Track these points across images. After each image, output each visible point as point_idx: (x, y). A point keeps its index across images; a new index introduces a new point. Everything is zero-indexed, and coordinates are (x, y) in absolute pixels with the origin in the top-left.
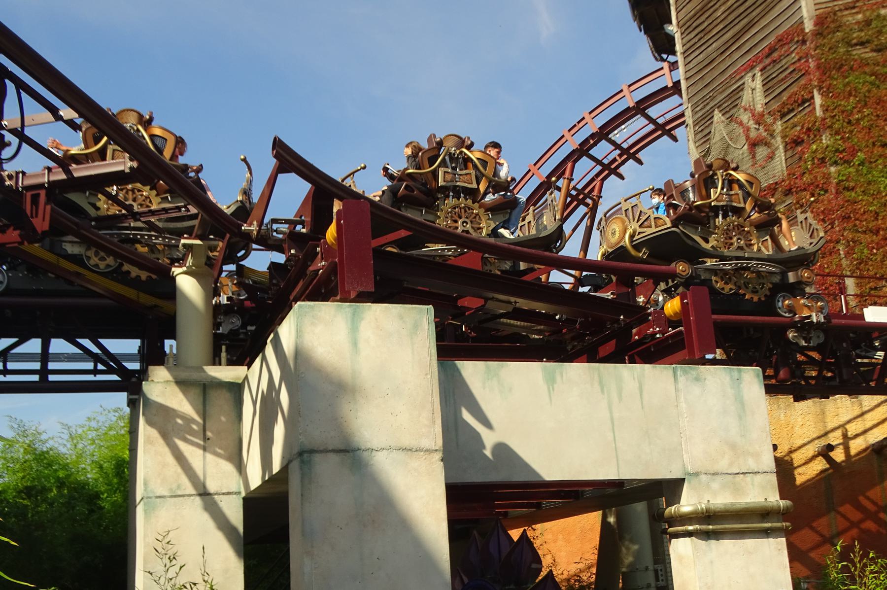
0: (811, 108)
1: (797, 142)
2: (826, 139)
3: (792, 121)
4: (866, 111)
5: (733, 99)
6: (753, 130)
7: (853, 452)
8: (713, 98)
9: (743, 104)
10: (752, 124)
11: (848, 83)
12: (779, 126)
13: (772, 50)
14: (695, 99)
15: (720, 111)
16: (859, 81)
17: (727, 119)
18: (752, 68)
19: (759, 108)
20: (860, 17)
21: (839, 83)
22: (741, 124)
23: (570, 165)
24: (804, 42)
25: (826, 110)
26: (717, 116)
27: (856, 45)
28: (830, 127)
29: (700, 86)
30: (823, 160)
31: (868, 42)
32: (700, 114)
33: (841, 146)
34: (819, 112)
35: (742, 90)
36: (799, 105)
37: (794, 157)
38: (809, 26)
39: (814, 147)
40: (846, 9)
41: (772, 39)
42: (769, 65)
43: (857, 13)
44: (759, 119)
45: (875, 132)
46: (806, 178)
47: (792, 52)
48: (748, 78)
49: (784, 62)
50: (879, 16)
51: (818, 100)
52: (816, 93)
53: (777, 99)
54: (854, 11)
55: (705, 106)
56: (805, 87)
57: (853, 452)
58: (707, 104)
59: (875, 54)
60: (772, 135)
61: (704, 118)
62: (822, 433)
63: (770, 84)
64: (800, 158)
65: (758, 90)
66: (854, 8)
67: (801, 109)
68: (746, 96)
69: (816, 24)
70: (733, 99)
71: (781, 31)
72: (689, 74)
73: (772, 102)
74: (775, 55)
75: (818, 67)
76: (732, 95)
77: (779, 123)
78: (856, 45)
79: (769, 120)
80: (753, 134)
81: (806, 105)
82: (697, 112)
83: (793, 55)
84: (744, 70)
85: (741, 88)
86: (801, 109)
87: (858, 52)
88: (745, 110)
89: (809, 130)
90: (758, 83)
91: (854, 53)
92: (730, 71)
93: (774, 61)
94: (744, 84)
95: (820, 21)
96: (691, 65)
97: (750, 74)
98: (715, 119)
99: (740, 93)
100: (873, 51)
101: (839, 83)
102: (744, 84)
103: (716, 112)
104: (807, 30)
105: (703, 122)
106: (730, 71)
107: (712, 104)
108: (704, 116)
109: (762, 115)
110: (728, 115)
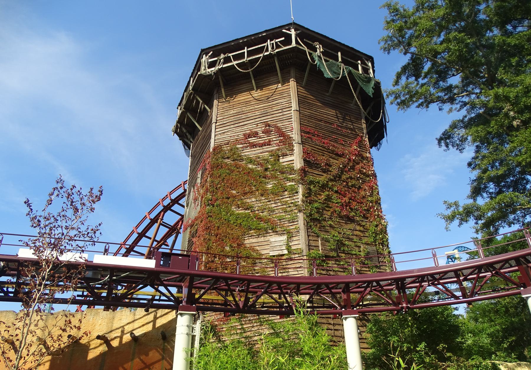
7: (124, 342)
23: (162, 213)
27: (226, 158)
57: (124, 342)
62: (110, 330)
78: (226, 158)
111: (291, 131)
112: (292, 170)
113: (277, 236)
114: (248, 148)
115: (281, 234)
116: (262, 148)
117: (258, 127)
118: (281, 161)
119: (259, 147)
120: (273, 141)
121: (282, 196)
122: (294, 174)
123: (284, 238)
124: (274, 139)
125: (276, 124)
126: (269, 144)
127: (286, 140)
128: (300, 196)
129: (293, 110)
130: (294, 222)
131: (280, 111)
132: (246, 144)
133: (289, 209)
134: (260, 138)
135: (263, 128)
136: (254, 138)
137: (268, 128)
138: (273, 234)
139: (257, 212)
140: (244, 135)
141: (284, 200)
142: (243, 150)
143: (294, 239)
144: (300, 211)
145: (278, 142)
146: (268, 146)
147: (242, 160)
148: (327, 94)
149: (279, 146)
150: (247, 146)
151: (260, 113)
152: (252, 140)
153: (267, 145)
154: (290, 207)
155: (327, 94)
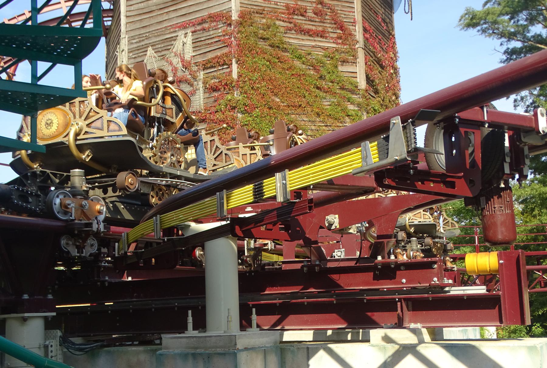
0: (228, 70)
1: (215, 89)
2: (237, 95)
3: (212, 74)
4: (264, 84)
5: (166, 44)
6: (179, 70)
8: (148, 38)
9: (174, 50)
10: (180, 66)
11: (255, 62)
12: (201, 75)
13: (203, 21)
14: (133, 34)
15: (153, 49)
16: (261, 63)
17: (159, 56)
18: (185, 28)
19: (188, 57)
20: (264, 21)
21: (249, 61)
22: (171, 64)
24: (230, 25)
25: (240, 76)
26: (150, 51)
27: (261, 38)
28: (242, 88)
29: (138, 25)
30: (234, 108)
31: (268, 39)
32: (135, 45)
33: (248, 102)
34: (235, 75)
35: (175, 40)
36: (219, 65)
37: (210, 99)
38: (235, 16)
39: (230, 98)
40: (257, 13)
41: (205, 13)
42: (199, 30)
43: (263, 18)
44: (186, 66)
45: (266, 97)
46: (219, 116)
47: (219, 28)
48: (181, 33)
49: (211, 33)
50: (275, 24)
51: (235, 66)
52: (234, 61)
53: (202, 55)
54: (262, 16)
55: (140, 41)
56: (226, 55)
58: (143, 40)
59: (270, 48)
60: (195, 78)
61: (138, 50)
63: (198, 44)
64: (215, 101)
65: (188, 45)
66: (262, 14)
67: (220, 68)
68: (178, 46)
69: (240, 17)
70: (166, 44)
71: (213, 11)
72: (129, 14)
73: (198, 56)
74: (206, 25)
75: (238, 45)
76: (165, 41)
77: (202, 73)
78: (261, 38)
79: (195, 68)
80: (180, 74)
81: (225, 67)
82: (132, 43)
83: (220, 31)
84: (179, 27)
85: (175, 39)
86: (220, 68)
87: (261, 44)
88: (176, 55)
89: (226, 84)
90: (189, 39)
91: (260, 43)
92: (165, 24)
93: (204, 30)
94: (177, 36)
95: (242, 15)
96: (132, 8)
97: (183, 32)
98: (148, 53)
99: (173, 42)
100: (270, 46)
101: (249, 61)
102: (177, 36)
103: (150, 49)
104: (233, 18)
105: (137, 52)
106: (165, 24)
107: (146, 42)
108: (139, 48)
109: (190, 63)
110: (160, 54)
111: (354, 23)
112: (354, 89)
114: (293, 32)
116: (312, 38)
118: (340, 68)
119: (310, 36)
120: (328, 32)
121: (341, 122)
124: (330, 30)
125: (334, 5)
126: (322, 35)
132: (290, 23)
134: (309, 20)
135: (314, 6)
136: (300, 17)
137: (320, 6)
140: (287, 7)
142: (286, 33)
147: (285, 50)
149: (337, 44)
150: (290, 30)
152: (298, 19)
153: (321, 37)
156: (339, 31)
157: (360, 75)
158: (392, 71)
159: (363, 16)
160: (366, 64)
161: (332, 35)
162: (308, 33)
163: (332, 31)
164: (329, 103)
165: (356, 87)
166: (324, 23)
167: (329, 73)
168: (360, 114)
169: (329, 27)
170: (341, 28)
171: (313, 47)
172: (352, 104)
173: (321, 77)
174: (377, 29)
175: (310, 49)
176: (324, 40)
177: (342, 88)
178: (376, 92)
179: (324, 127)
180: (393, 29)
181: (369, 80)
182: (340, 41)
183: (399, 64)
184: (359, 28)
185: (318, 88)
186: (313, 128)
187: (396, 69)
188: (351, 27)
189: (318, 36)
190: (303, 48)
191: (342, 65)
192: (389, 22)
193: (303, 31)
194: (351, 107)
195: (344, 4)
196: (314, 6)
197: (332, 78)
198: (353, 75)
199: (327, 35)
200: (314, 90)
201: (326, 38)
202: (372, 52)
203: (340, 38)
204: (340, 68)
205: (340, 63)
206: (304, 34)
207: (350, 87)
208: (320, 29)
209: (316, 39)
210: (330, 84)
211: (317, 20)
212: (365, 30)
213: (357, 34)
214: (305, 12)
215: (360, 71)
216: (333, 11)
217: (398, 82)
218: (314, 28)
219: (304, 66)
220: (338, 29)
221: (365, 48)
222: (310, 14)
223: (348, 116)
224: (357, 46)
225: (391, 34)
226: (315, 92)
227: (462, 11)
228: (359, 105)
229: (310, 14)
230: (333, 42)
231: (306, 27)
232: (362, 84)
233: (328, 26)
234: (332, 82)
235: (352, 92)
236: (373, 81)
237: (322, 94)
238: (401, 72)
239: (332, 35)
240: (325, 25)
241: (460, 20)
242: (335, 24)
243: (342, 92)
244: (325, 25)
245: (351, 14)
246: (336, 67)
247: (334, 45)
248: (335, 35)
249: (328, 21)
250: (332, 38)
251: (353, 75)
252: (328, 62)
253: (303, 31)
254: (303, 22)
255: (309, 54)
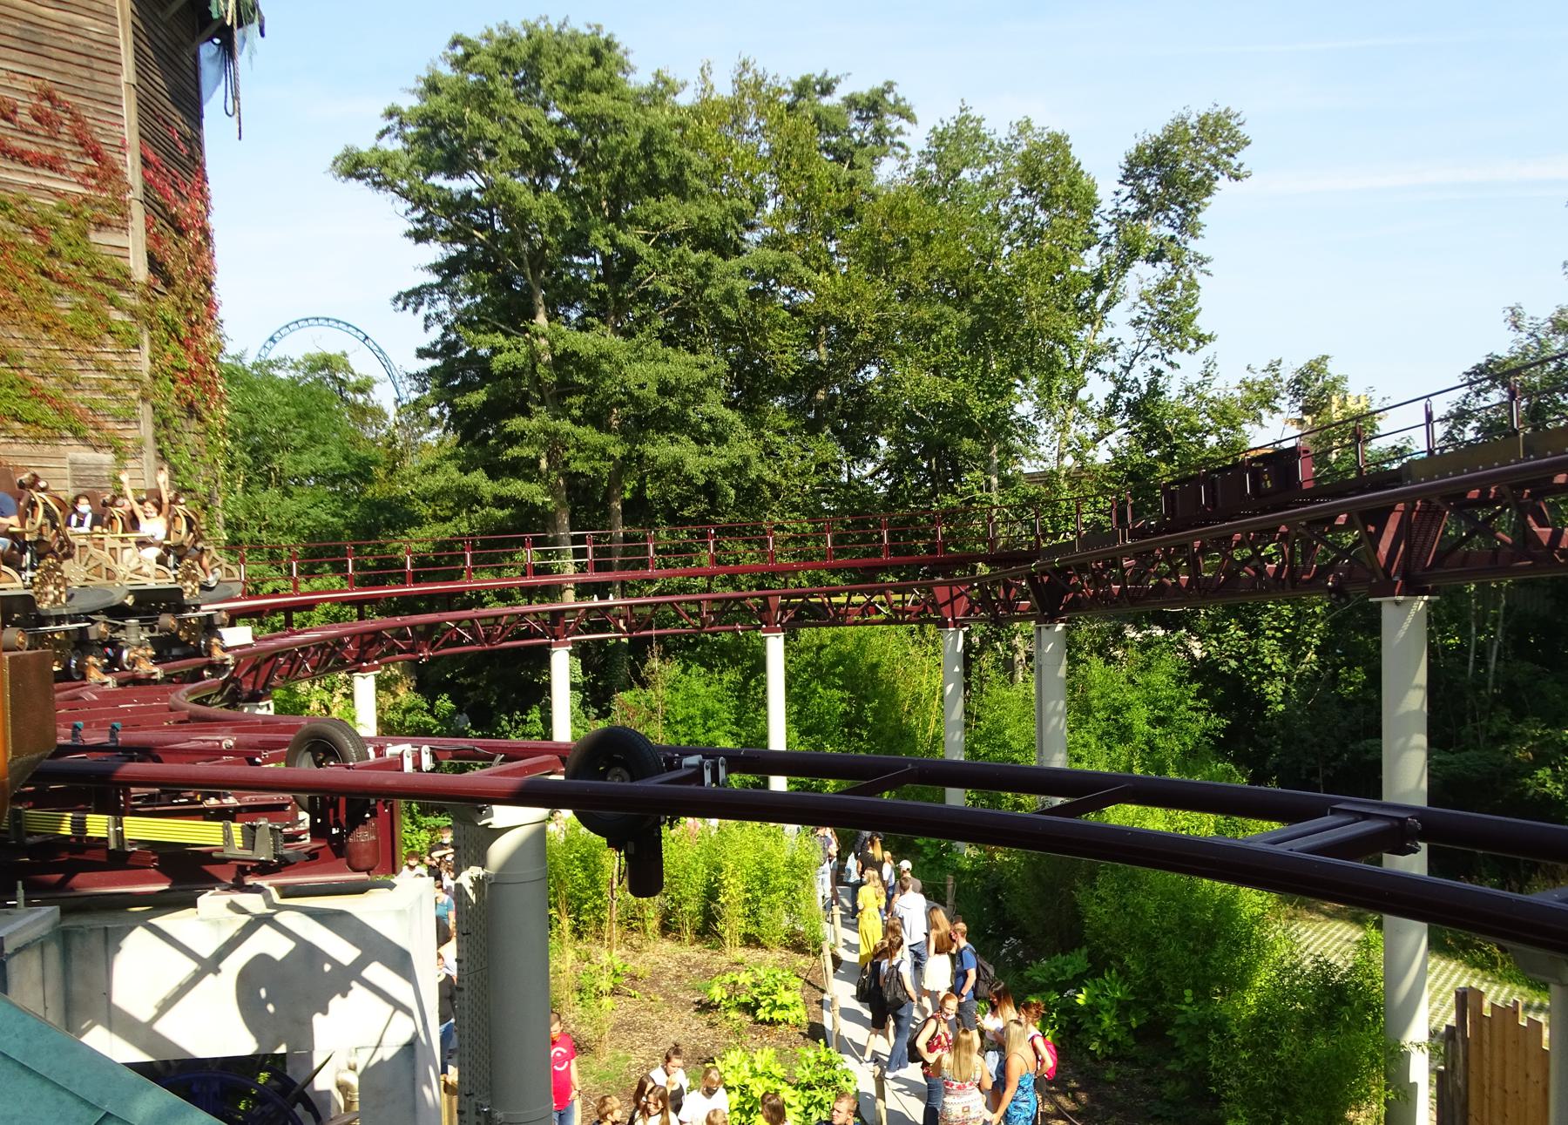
111: (122, 148)
112: (123, 281)
113: (86, 449)
115: (96, 448)
117: (16, 85)
118: (94, 237)
119: (26, 163)
120: (66, 161)
121: (96, 345)
122: (128, 291)
123: (107, 457)
126: (53, 164)
127: (107, 174)
128: (143, 362)
129: (124, 78)
130: (126, 422)
131: (84, 60)
133: (118, 386)
137: (46, 104)
138: (75, 442)
139: (27, 372)
141: (104, 357)
143: (130, 463)
144: (144, 399)
145: (81, 169)
146: (47, 173)
148: (159, 14)
149: (87, 186)
151: (16, 33)
153: (51, 168)
154: (118, 380)
155: (159, 14)
156: (91, 161)
157: (135, 253)
158: (199, 238)
159: (141, 134)
160: (147, 231)
161: (74, 168)
162: (21, 156)
163: (75, 158)
164: (69, 305)
165: (128, 277)
166: (57, 140)
167: (70, 245)
168: (135, 330)
169: (69, 151)
170: (96, 155)
171: (33, 187)
172: (118, 309)
173: (51, 253)
174: (170, 155)
175: (25, 193)
176: (58, 176)
177: (98, 278)
178: (169, 282)
179: (58, 353)
180: (202, 153)
181: (155, 264)
182: (93, 182)
183: (213, 221)
184: (133, 159)
185: (44, 273)
186: (37, 353)
187: (206, 233)
188: (116, 156)
189: (42, 165)
190: (9, 188)
191: (98, 231)
192: (195, 143)
193: (9, 152)
194: (116, 316)
195: (100, 107)
196: (35, 101)
197: (76, 256)
198: (120, 252)
199: (65, 166)
200: (34, 277)
201: (62, 172)
202: (159, 205)
203: (94, 176)
204: (94, 237)
205: (92, 226)
206: (13, 159)
207: (115, 275)
208: (49, 152)
209: (38, 171)
210: (72, 267)
211: (41, 132)
212: (146, 162)
213: (128, 170)
214: (14, 112)
215: (135, 245)
216: (76, 119)
217: (212, 256)
218: (33, 148)
219: (12, 226)
220: (88, 155)
221: (148, 201)
222: (25, 118)
223: (110, 332)
224: (129, 196)
225: (197, 162)
226: (37, 282)
227: (339, 151)
228: (133, 313)
229: (25, 118)
230: (78, 183)
231: (15, 144)
232: (140, 270)
233: (67, 147)
234: (75, 264)
235: (120, 286)
236: (161, 264)
237: (53, 286)
238: (218, 237)
239: (74, 168)
240: (58, 145)
241: (335, 163)
242: (82, 145)
243: (100, 286)
244: (58, 145)
245: (116, 128)
246: (84, 234)
247: (81, 190)
248: (81, 169)
249: (66, 138)
250: (75, 174)
251: (120, 252)
252: (67, 222)
253: (9, 152)
254: (10, 132)
255: (24, 202)
